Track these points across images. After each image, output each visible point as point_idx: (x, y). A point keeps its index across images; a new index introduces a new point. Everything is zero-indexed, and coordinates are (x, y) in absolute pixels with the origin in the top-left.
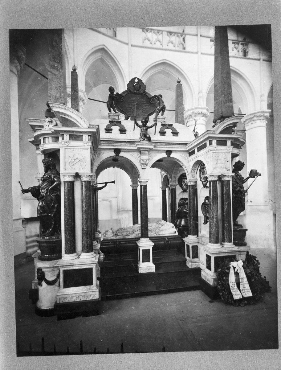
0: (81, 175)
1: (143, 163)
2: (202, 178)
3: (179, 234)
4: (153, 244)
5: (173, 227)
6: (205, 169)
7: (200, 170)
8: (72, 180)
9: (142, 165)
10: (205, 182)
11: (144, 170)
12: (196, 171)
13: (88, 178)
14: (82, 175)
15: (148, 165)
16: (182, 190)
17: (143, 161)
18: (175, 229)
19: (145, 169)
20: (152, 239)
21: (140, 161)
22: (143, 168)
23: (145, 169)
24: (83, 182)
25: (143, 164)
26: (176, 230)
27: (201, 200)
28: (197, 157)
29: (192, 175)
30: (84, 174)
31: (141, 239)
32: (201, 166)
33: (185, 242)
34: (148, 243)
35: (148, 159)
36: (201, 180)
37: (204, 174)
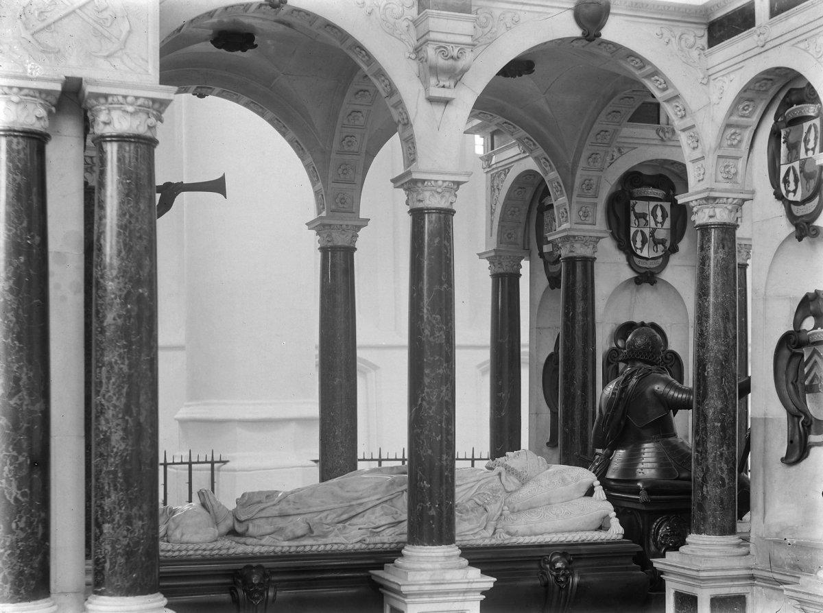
0: (97, 96)
1: (441, 62)
2: (786, 181)
3: (625, 536)
4: (488, 582)
5: (590, 492)
6: (806, 125)
7: (775, 135)
8: (38, 126)
9: (433, 81)
10: (804, 202)
11: (438, 110)
12: (747, 135)
13: (144, 116)
14: (106, 96)
15: (467, 77)
16: (629, 274)
17: (442, 49)
18: (601, 505)
19: (446, 102)
20: (478, 557)
21: (417, 50)
22: (432, 100)
23: (446, 102)
24: (101, 140)
25: (435, 71)
26: (608, 508)
27: (767, 324)
28: (764, 49)
29: (722, 162)
30: (123, 92)
31: (408, 550)
32: (786, 104)
33: (663, 582)
34: (457, 575)
35: (468, 40)
36: (779, 196)
37: (803, 155)
